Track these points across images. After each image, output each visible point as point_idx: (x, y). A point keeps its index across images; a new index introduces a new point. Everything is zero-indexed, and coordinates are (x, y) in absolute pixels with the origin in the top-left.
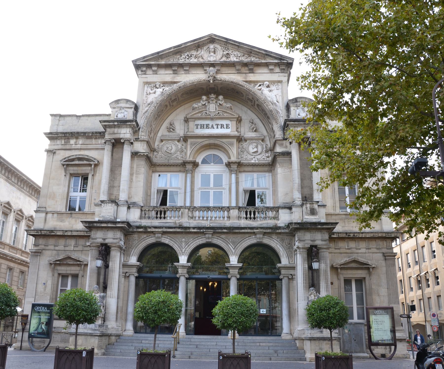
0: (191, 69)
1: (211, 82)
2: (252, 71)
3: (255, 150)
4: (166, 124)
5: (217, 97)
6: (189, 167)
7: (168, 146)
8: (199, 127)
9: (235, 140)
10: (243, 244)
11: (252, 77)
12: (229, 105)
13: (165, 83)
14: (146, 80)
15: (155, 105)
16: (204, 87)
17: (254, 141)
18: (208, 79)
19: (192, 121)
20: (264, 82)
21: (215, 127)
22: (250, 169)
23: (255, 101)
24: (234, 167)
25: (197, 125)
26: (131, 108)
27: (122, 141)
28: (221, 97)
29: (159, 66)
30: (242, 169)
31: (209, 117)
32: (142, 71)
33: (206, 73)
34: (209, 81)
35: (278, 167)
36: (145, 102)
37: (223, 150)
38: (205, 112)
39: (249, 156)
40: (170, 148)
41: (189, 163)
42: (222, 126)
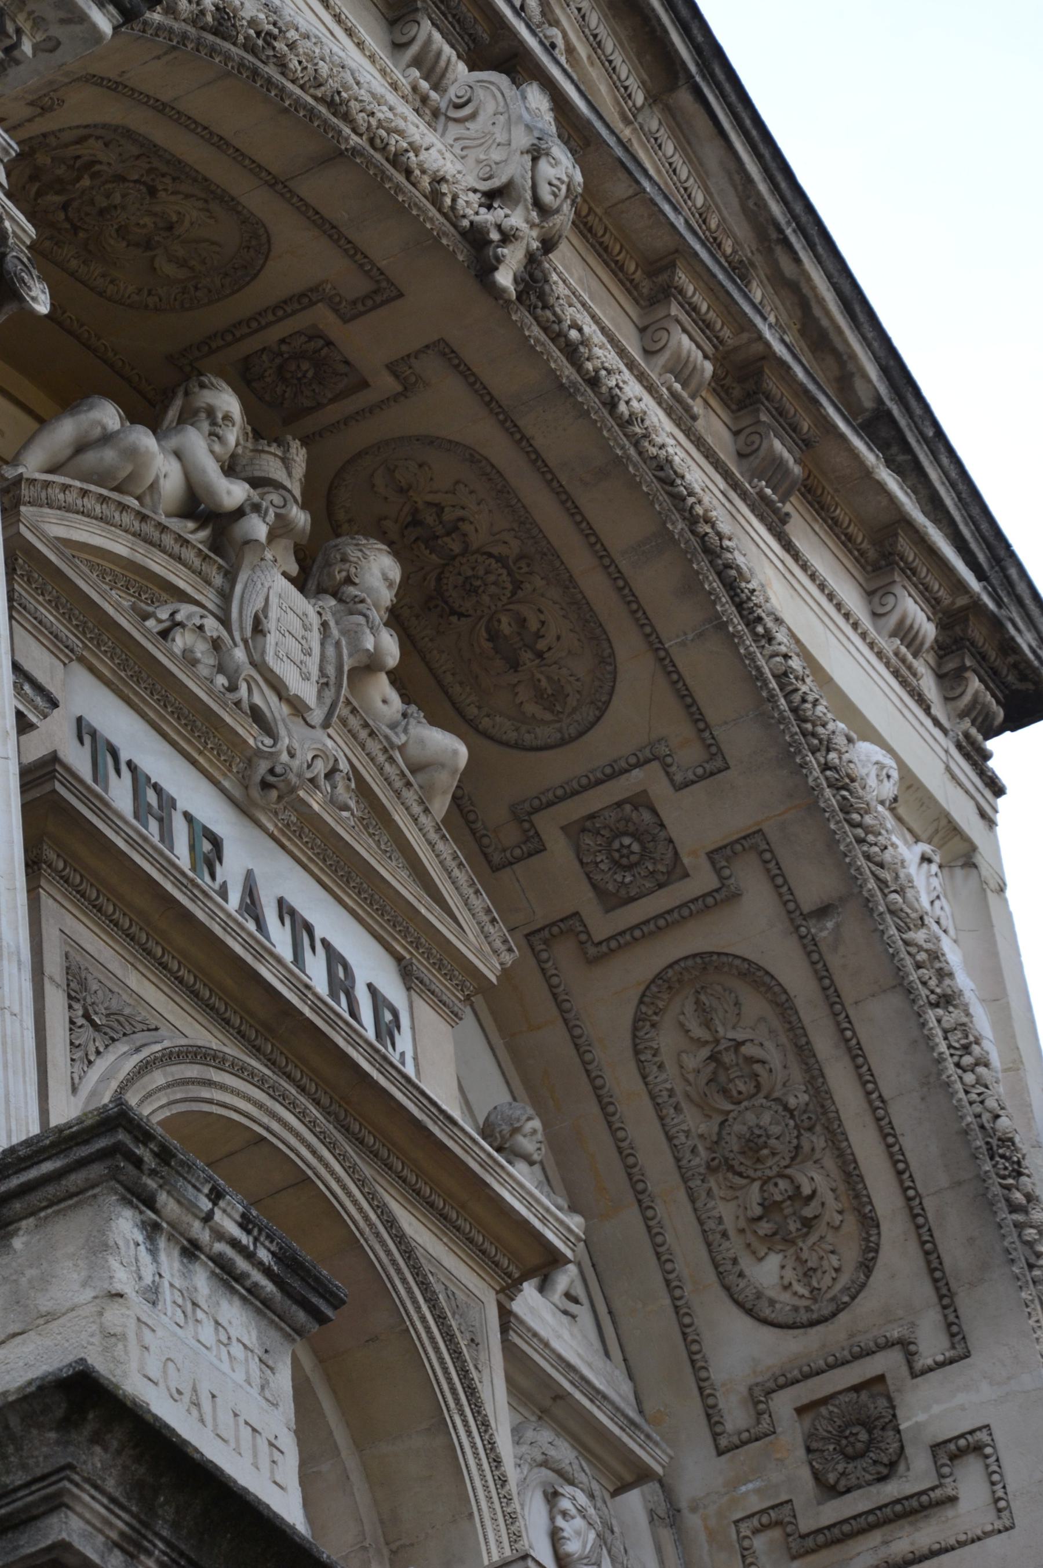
31: (250, 735)
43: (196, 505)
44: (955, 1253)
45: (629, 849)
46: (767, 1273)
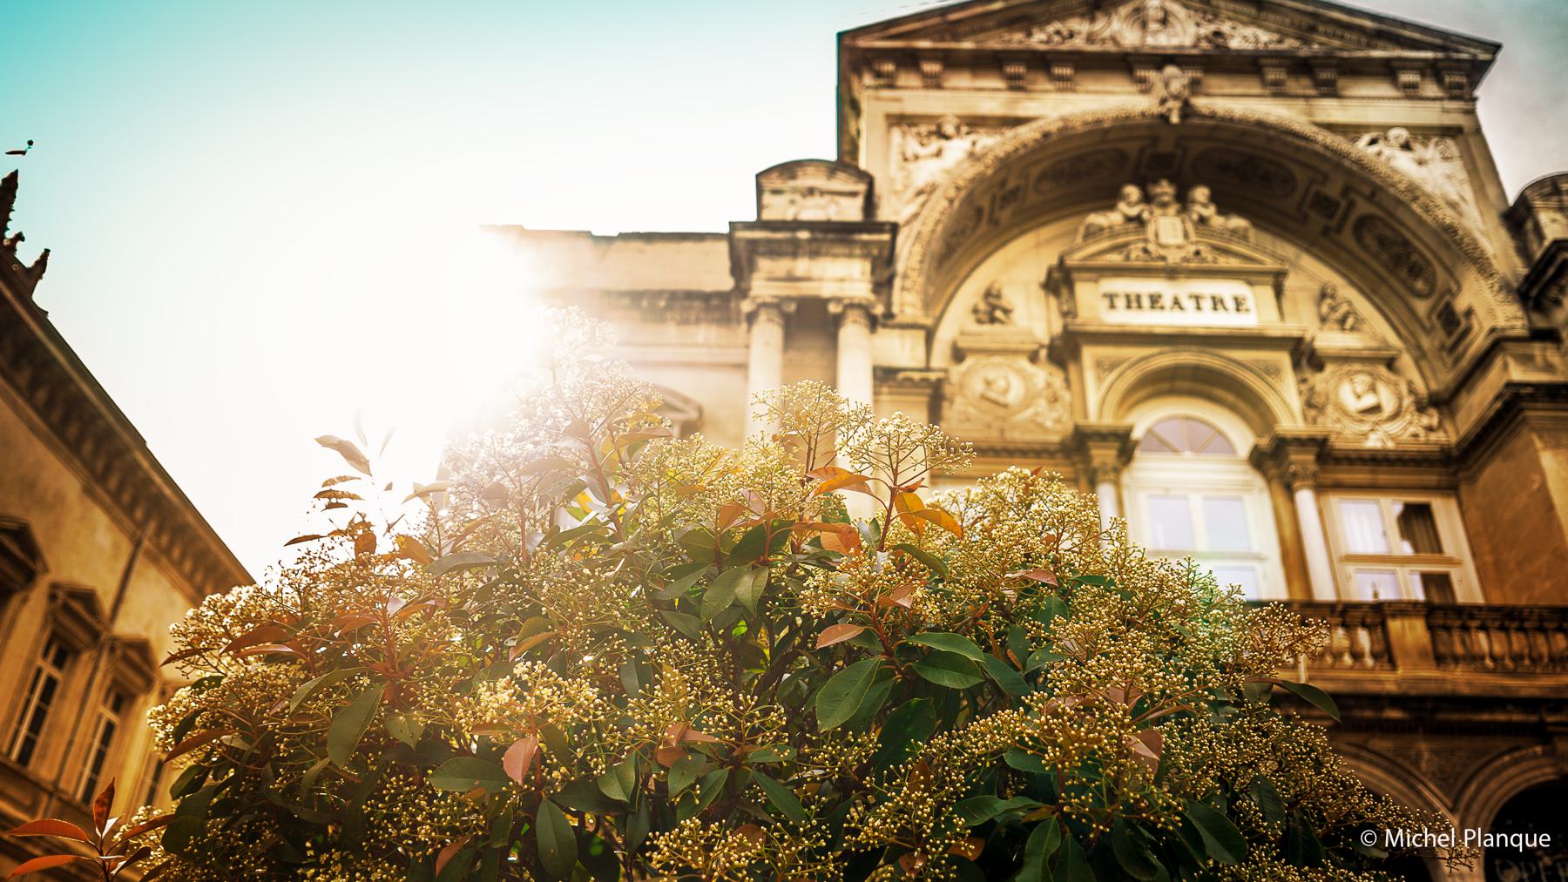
0: (1079, 78)
1: (1175, 119)
2: (1330, 91)
3: (1369, 400)
4: (969, 294)
5: (1183, 200)
6: (1103, 455)
7: (991, 375)
8: (1121, 302)
9: (1284, 359)
10: (1493, 785)
11: (1331, 110)
12: (1237, 222)
13: (975, 123)
14: (895, 109)
15: (952, 193)
16: (1132, 148)
17: (1357, 367)
18: (1163, 110)
19: (1089, 280)
20: (1386, 128)
21: (1189, 304)
22: (1362, 476)
23: (1351, 205)
24: (1303, 460)
25: (1111, 298)
26: (854, 194)
27: (833, 308)
28: (1201, 193)
29: (952, 62)
30: (1330, 477)
31: (1161, 264)
32: (878, 75)
33: (1145, 92)
34: (1164, 118)
35: (1539, 444)
36: (899, 187)
37: (1231, 398)
38: (1141, 245)
39: (1346, 421)
40: (1001, 383)
41: (1103, 436)
42: (1217, 302)
43: (1129, 219)
44: (1448, 263)
45: (1325, 205)
46: (1420, 285)
